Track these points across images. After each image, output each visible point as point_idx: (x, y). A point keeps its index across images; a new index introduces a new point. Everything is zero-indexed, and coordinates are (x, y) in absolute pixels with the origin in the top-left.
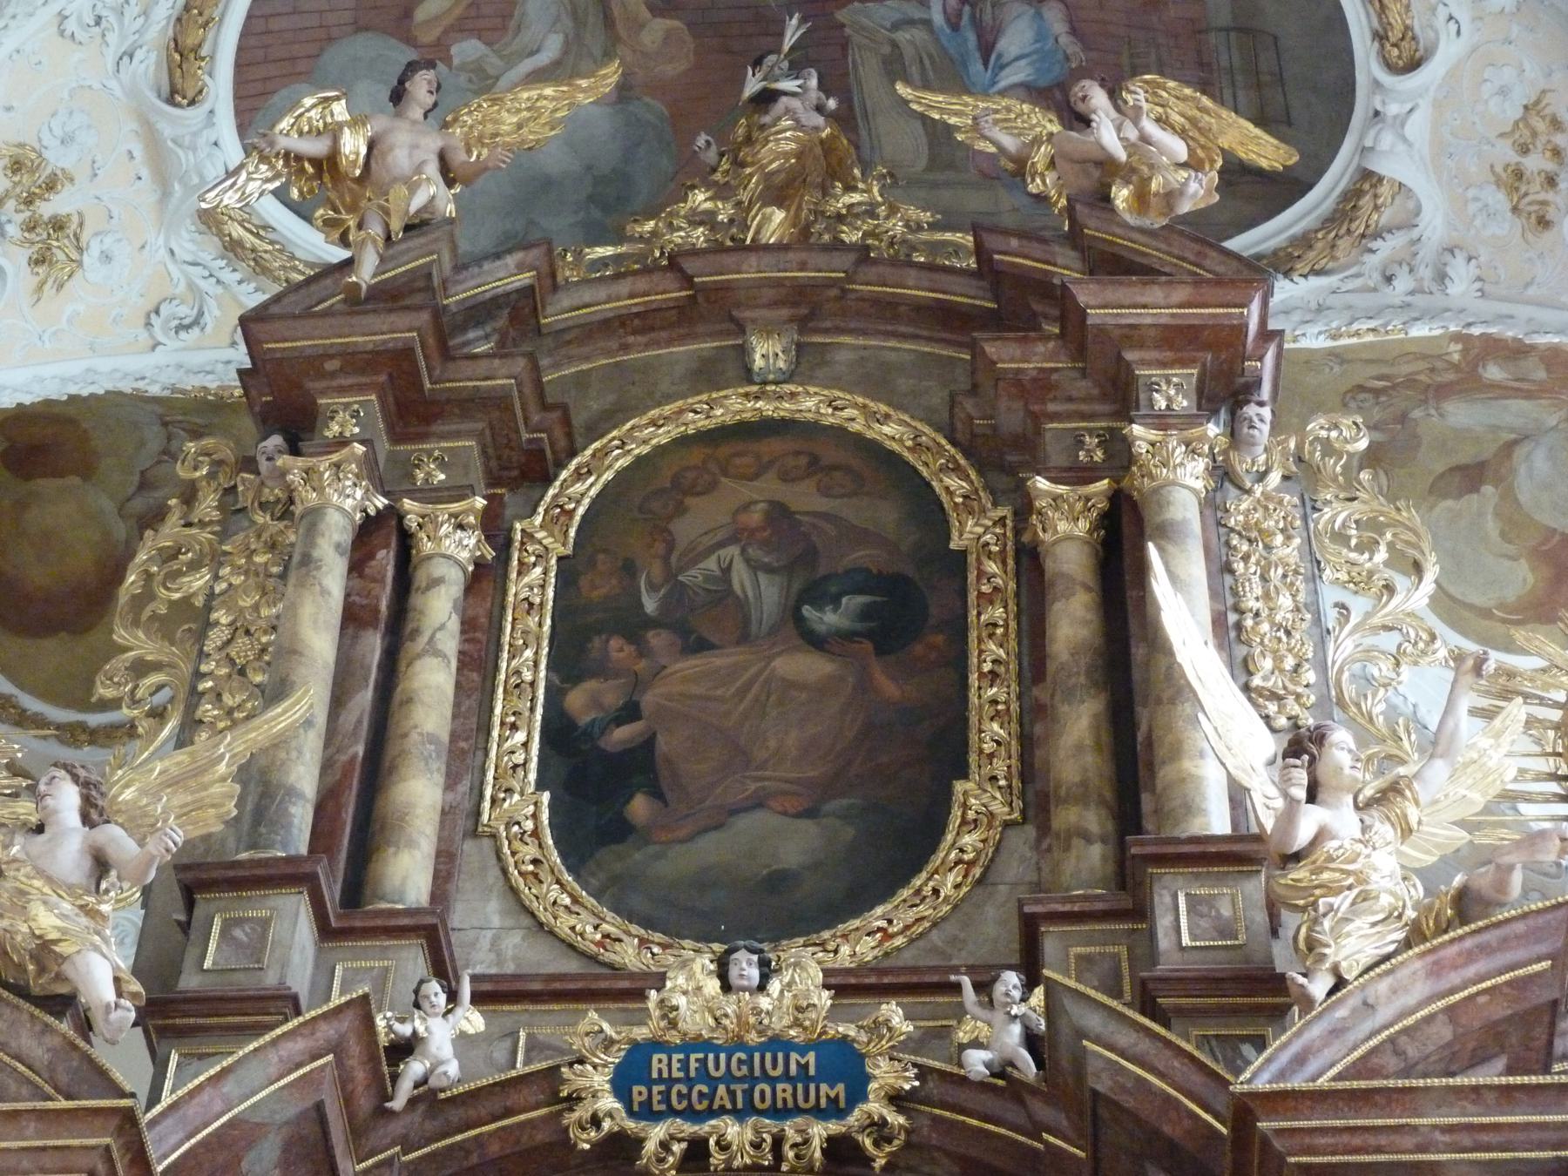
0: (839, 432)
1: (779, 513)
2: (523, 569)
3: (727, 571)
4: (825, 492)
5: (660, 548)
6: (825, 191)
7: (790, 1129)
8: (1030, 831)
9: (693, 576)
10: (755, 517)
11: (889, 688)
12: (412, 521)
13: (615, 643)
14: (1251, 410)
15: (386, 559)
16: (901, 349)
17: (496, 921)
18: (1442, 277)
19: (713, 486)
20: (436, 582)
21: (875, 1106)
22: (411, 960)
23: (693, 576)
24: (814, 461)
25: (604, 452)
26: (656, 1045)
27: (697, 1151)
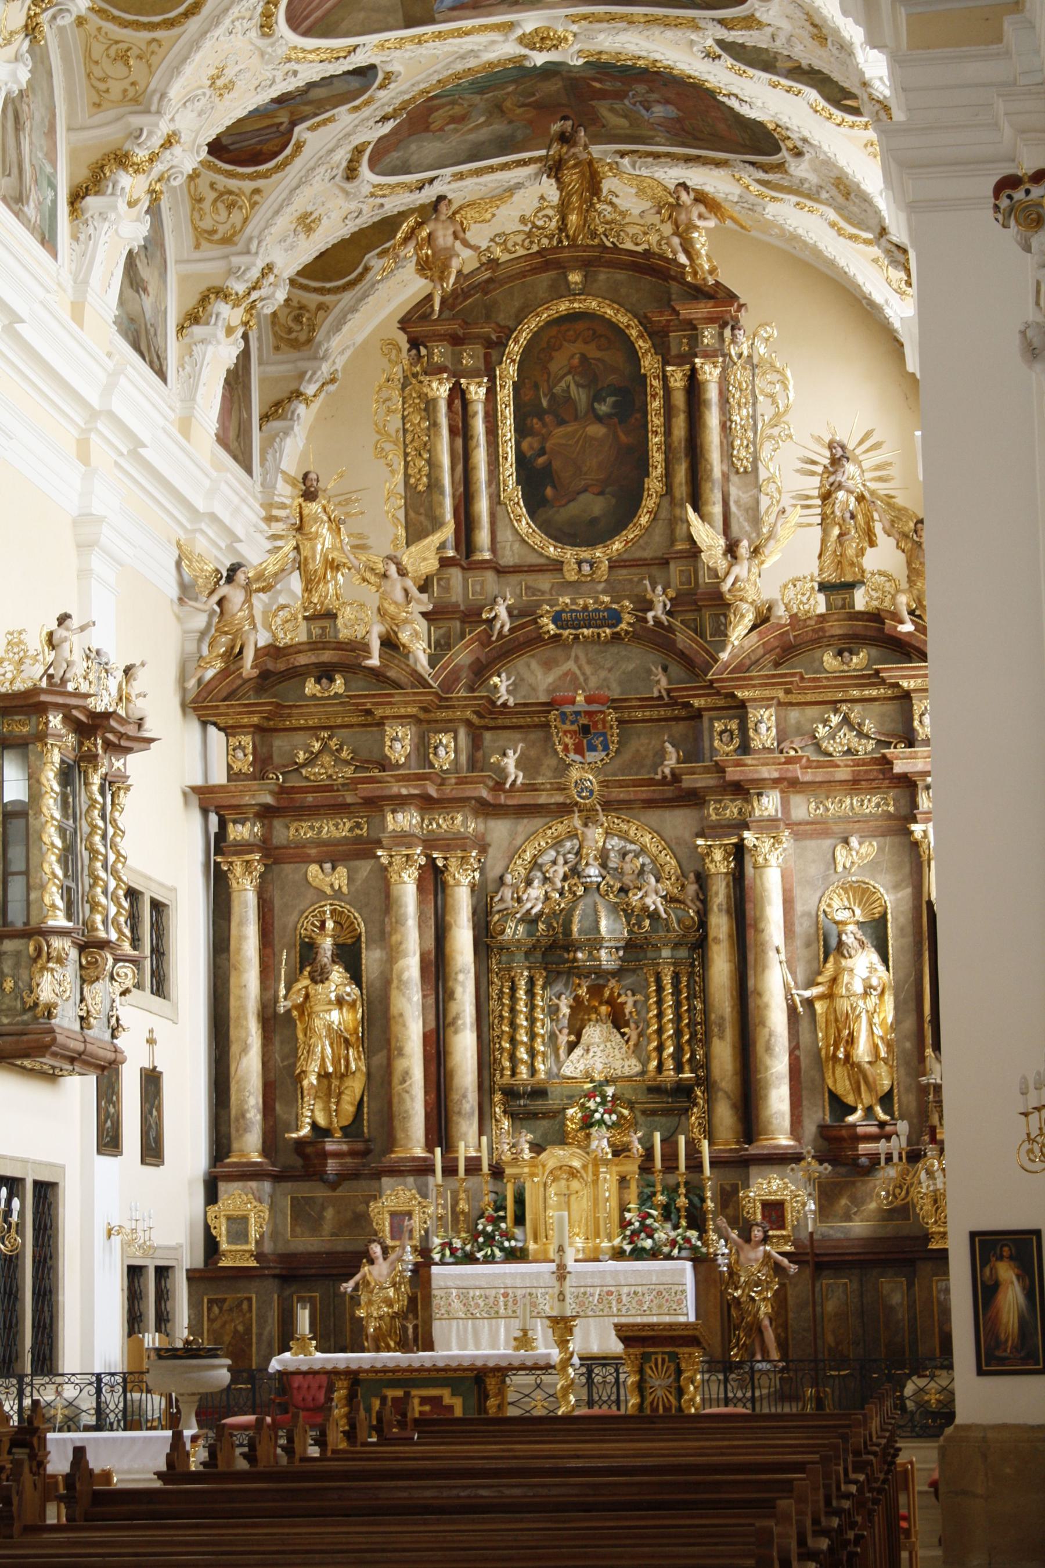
0: (602, 319)
1: (584, 358)
2: (502, 387)
3: (568, 387)
4: (599, 348)
5: (545, 377)
6: (592, 205)
7: (600, 631)
8: (667, 499)
9: (557, 390)
10: (576, 361)
11: (623, 437)
12: (464, 386)
13: (535, 421)
14: (737, 332)
15: (458, 402)
16: (621, 276)
17: (511, 538)
18: (818, 193)
19: (561, 347)
20: (476, 413)
21: (623, 626)
22: (490, 576)
23: (557, 390)
24: (595, 332)
25: (521, 332)
26: (563, 611)
27: (576, 637)
